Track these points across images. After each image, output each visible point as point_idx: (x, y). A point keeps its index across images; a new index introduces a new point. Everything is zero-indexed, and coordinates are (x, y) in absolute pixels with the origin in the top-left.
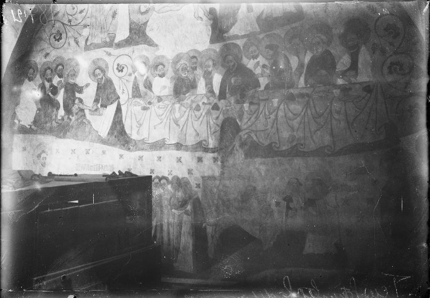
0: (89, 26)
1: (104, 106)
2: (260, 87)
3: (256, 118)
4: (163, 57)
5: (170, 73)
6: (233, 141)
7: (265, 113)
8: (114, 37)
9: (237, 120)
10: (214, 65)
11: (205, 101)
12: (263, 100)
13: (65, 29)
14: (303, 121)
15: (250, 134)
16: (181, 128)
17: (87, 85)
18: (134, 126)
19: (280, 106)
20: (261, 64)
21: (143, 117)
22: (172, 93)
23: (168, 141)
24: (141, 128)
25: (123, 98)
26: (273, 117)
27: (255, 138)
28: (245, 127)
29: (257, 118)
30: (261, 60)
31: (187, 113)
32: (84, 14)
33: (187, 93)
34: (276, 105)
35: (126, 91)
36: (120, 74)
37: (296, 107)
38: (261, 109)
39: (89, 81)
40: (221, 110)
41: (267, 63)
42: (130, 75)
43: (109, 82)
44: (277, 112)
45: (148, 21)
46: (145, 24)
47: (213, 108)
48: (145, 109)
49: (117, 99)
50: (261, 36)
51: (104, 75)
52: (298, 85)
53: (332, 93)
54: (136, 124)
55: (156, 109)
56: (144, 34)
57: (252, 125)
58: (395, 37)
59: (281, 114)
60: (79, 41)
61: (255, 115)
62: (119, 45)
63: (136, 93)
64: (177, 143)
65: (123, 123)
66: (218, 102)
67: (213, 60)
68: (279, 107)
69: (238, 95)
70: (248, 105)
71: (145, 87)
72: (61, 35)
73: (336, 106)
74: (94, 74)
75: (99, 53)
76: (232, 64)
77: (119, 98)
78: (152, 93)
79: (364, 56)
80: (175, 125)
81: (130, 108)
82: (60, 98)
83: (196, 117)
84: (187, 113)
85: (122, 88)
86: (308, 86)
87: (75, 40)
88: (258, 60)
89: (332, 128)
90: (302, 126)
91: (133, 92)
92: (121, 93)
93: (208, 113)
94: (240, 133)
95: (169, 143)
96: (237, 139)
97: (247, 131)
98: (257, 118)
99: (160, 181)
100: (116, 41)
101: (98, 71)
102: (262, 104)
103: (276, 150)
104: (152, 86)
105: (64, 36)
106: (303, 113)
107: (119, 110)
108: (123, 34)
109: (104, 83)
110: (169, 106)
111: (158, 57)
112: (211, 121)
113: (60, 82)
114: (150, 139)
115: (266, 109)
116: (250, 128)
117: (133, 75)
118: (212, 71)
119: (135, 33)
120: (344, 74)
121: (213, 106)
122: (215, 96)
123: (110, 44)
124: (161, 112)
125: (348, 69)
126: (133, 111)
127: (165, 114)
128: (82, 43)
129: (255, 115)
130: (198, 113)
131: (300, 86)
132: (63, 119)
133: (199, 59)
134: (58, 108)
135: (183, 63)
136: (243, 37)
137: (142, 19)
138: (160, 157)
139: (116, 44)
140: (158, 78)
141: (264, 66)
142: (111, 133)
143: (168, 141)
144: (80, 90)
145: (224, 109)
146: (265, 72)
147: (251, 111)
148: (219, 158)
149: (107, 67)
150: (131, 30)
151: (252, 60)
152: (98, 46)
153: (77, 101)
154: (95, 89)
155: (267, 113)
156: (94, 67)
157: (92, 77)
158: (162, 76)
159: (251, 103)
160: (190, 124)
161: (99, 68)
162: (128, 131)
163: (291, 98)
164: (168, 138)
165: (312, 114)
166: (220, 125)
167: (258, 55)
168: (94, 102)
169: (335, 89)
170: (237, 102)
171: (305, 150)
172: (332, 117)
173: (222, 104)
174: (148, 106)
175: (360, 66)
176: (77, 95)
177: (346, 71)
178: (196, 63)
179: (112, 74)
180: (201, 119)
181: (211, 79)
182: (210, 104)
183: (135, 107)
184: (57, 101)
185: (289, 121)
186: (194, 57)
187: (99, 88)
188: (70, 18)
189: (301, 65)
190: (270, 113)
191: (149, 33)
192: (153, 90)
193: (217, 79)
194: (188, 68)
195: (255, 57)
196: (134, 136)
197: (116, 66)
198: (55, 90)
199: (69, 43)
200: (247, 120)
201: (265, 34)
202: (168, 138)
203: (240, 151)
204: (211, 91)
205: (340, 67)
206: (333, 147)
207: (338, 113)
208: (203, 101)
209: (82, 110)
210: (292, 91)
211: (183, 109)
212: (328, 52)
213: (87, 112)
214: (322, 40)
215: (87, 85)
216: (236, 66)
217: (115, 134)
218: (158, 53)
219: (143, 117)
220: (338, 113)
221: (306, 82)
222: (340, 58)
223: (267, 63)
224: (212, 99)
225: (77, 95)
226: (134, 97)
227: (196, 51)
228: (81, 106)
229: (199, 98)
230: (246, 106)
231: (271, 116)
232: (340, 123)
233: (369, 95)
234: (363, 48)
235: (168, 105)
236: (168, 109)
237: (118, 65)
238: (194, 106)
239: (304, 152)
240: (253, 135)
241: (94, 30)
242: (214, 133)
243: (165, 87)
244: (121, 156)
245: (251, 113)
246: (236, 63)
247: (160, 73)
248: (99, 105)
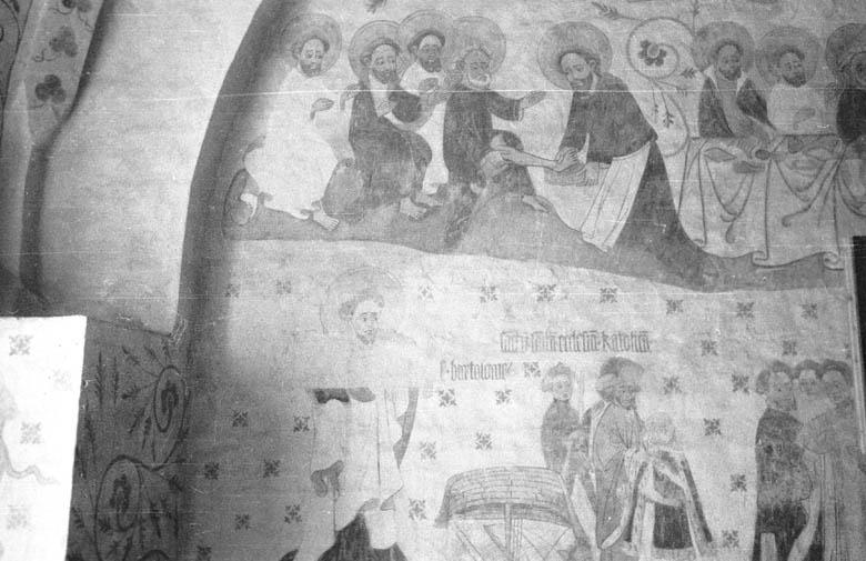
4: (794, 31)
5: (825, 75)
17: (536, 97)
18: (713, 220)
21: (743, 194)
24: (738, 223)
25: (668, 137)
35: (678, 117)
39: (542, 84)
42: (689, 73)
49: (649, 138)
55: (785, 170)
71: (745, 110)
77: (651, 136)
78: (767, 129)
82: (432, 130)
85: (662, 110)
91: (703, 123)
92: (660, 122)
99: (820, 376)
101: (572, 59)
104: (765, 108)
107: (655, 169)
111: (777, 31)
113: (431, 83)
117: (698, 74)
124: (802, 178)
127: (816, 187)
132: (442, 192)
134: (424, 157)
135: (859, 49)
138: (814, 307)
142: (632, 234)
153: (496, 142)
154: (566, 110)
157: (556, 76)
158: (797, 81)
162: (692, 232)
174: (757, 161)
176: (498, 123)
183: (712, 165)
184: (419, 138)
187: (578, 107)
196: (716, 245)
197: (636, 49)
198: (409, 107)
209: (520, 169)
213: (537, 175)
215: (536, 97)
225: (498, 123)
226: (705, 134)
228: (517, 158)
236: (825, 172)
237: (645, 44)
244: (673, 306)
248: (582, 156)
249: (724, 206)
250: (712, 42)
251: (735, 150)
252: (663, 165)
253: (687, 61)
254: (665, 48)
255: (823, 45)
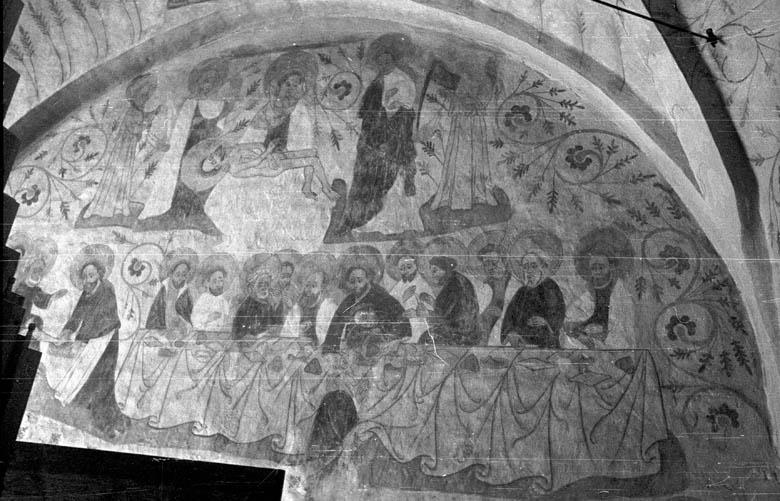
0: (96, 183)
1: (84, 338)
2: (410, 335)
3: (396, 397)
4: (227, 256)
5: (235, 288)
6: (337, 443)
7: (414, 391)
8: (140, 211)
9: (354, 399)
10: (325, 282)
11: (295, 352)
12: (412, 363)
13: (49, 184)
14: (491, 415)
15: (377, 431)
16: (234, 401)
17: (61, 294)
19: (445, 379)
20: (418, 291)
21: (158, 372)
22: (230, 328)
23: (199, 427)
24: (148, 394)
25: (127, 326)
26: (429, 400)
27: (386, 442)
28: (370, 415)
29: (397, 398)
30: (420, 284)
31: (251, 373)
32: (94, 162)
33: (260, 332)
34: (438, 376)
35: (136, 315)
36: (133, 280)
37: (481, 384)
38: (407, 381)
39: (67, 285)
40: (323, 373)
41: (430, 291)
42: (153, 282)
43: (109, 292)
44: (440, 392)
45: (211, 189)
46: (205, 193)
47: (308, 370)
48: (165, 353)
50: (427, 239)
51: (101, 276)
52: (487, 341)
53: (555, 365)
54: (141, 382)
55: (190, 357)
56: (199, 209)
57: (383, 413)
58: (679, 272)
59: (446, 396)
60: (71, 208)
61: (393, 392)
62: (145, 226)
63: (157, 320)
64: (219, 434)
65: (113, 381)
66: (319, 357)
67: (324, 273)
68: (443, 383)
69: (364, 347)
70: (381, 370)
71: (178, 311)
72: (38, 193)
73: (562, 391)
74: (81, 274)
75: (104, 235)
76: (361, 285)
77: (118, 325)
78: (188, 325)
79: (621, 297)
80: (221, 395)
81: (136, 349)
83: (269, 383)
84: (251, 373)
85: (129, 308)
86: (509, 344)
87: (62, 206)
88: (414, 283)
89: (549, 439)
90: (488, 425)
91: (150, 318)
92: (125, 316)
93: (296, 377)
94: (356, 429)
95: (201, 433)
96: (349, 438)
97: (372, 425)
98: (397, 398)
100: (143, 216)
102: (411, 371)
103: (428, 472)
104: (191, 311)
105: (42, 196)
106: (492, 400)
107: (112, 350)
108: (158, 204)
109: (97, 293)
110: (219, 354)
112: (299, 395)
114: (162, 420)
115: (418, 382)
116: (379, 419)
117: (159, 284)
118: (318, 294)
119: (183, 207)
120: (577, 331)
121: (308, 366)
122: (316, 344)
123: (133, 219)
124: (197, 364)
125: (589, 322)
126: (140, 357)
128: (75, 211)
129: (393, 392)
130: (275, 377)
131: (490, 344)
133: (297, 269)
136: (389, 237)
137: (198, 183)
139: (140, 222)
140: (206, 296)
141: (424, 296)
142: (80, 399)
143: (199, 427)
144: (44, 302)
145: (331, 372)
146: (424, 309)
147: (386, 385)
148: (303, 478)
149: (111, 261)
150: (175, 200)
151: (401, 282)
152: (106, 222)
154: (75, 303)
155: (418, 391)
156: (84, 258)
157: (76, 278)
158: (215, 292)
159: (387, 367)
160: (253, 397)
161: (95, 264)
163: (473, 365)
164: (202, 422)
165: (510, 402)
166: (317, 408)
167: (414, 274)
168: (66, 327)
169: (562, 356)
170: (360, 361)
171: (490, 481)
172: (552, 415)
173: (328, 362)
175: (612, 317)
177: (585, 324)
178: (289, 276)
179: (116, 278)
180: (278, 388)
181: (317, 308)
182: (304, 359)
185: (461, 413)
186: (288, 264)
187: (82, 302)
188: (66, 166)
189: (497, 302)
190: (425, 393)
191: (210, 210)
192: (192, 318)
193: (326, 311)
194: (273, 284)
195: (407, 278)
196: (130, 408)
197: (128, 264)
199: (49, 211)
200: (376, 400)
201: (433, 237)
202: (202, 422)
203: (351, 467)
204: (311, 333)
205: (572, 316)
206: (549, 478)
207: (566, 407)
208: (290, 351)
210: (474, 350)
211: (246, 364)
212: (550, 285)
214: (541, 261)
216: (367, 291)
217: (91, 400)
218: (217, 248)
219: (158, 372)
220: (566, 407)
221: (503, 337)
222: (575, 297)
223: (430, 291)
224: (309, 349)
226: (149, 326)
227: (294, 253)
229: (283, 344)
230: (376, 372)
231: (426, 398)
232: (567, 429)
233: (628, 377)
234: (619, 283)
235: (216, 352)
236: (214, 360)
237: (135, 261)
238: (270, 358)
239: (487, 485)
240: (383, 435)
241: (105, 192)
242: (301, 421)
243: (218, 315)
245: (386, 387)
246: (370, 286)
247: (214, 287)
248: (73, 336)
249: (144, 380)
250: (171, 263)
251: (163, 340)
252: (117, 349)
253: (155, 274)
254: (146, 265)
255: (241, 267)
